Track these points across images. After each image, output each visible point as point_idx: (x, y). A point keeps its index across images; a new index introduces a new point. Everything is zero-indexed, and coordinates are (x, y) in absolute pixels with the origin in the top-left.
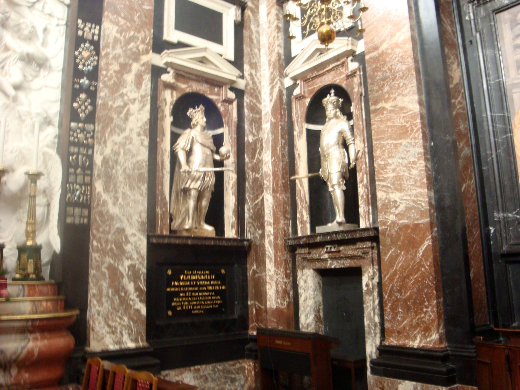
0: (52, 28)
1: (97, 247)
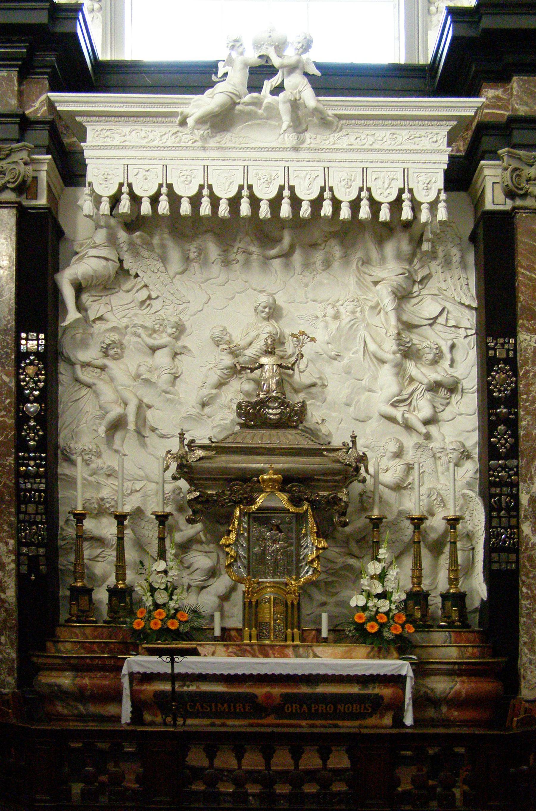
0: (461, 342)
1: (527, 593)
